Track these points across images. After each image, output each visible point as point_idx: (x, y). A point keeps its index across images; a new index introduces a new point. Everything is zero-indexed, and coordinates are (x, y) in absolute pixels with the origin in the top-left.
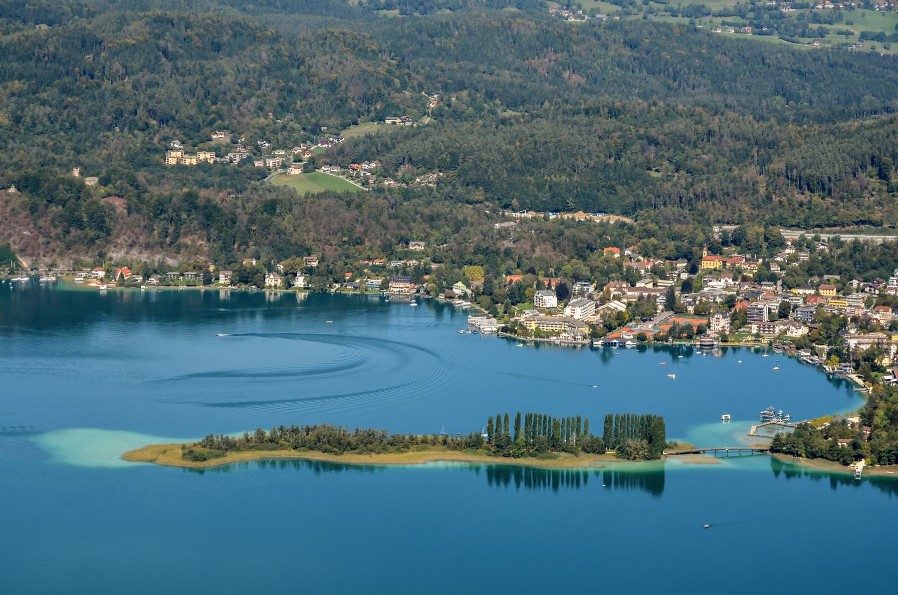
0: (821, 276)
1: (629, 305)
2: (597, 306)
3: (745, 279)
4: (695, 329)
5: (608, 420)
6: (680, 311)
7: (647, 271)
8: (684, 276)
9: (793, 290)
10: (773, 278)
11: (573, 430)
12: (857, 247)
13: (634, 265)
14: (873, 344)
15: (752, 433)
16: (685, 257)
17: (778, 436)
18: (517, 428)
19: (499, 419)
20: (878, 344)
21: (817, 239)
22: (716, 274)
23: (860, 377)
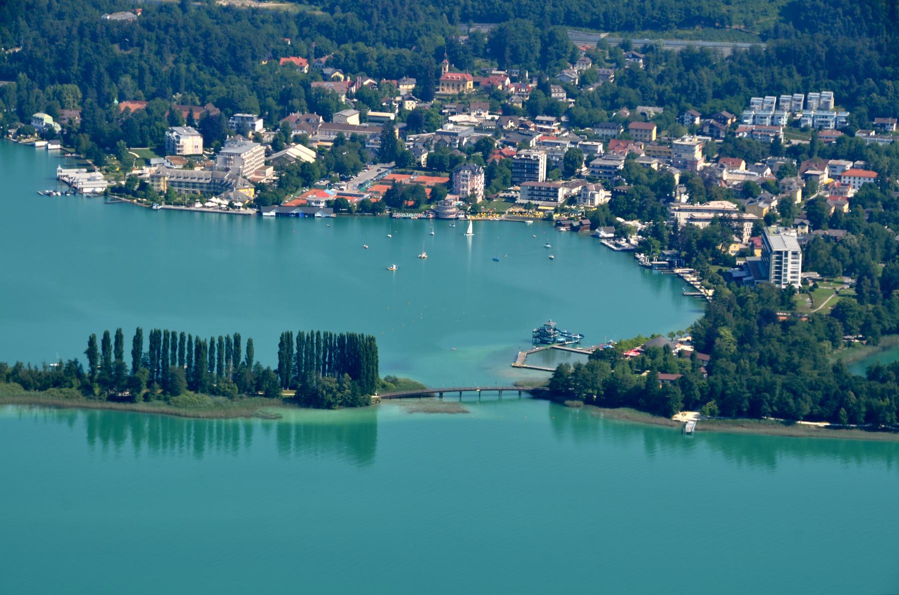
0: (631, 106)
1: (320, 152)
2: (268, 153)
3: (508, 111)
4: (428, 191)
5: (285, 341)
6: (404, 162)
7: (349, 96)
8: (410, 105)
10: (553, 110)
11: (228, 358)
12: (690, 60)
13: (327, 85)
14: (713, 221)
15: (518, 363)
18: (136, 353)
19: (106, 336)
20: (721, 219)
21: (626, 46)
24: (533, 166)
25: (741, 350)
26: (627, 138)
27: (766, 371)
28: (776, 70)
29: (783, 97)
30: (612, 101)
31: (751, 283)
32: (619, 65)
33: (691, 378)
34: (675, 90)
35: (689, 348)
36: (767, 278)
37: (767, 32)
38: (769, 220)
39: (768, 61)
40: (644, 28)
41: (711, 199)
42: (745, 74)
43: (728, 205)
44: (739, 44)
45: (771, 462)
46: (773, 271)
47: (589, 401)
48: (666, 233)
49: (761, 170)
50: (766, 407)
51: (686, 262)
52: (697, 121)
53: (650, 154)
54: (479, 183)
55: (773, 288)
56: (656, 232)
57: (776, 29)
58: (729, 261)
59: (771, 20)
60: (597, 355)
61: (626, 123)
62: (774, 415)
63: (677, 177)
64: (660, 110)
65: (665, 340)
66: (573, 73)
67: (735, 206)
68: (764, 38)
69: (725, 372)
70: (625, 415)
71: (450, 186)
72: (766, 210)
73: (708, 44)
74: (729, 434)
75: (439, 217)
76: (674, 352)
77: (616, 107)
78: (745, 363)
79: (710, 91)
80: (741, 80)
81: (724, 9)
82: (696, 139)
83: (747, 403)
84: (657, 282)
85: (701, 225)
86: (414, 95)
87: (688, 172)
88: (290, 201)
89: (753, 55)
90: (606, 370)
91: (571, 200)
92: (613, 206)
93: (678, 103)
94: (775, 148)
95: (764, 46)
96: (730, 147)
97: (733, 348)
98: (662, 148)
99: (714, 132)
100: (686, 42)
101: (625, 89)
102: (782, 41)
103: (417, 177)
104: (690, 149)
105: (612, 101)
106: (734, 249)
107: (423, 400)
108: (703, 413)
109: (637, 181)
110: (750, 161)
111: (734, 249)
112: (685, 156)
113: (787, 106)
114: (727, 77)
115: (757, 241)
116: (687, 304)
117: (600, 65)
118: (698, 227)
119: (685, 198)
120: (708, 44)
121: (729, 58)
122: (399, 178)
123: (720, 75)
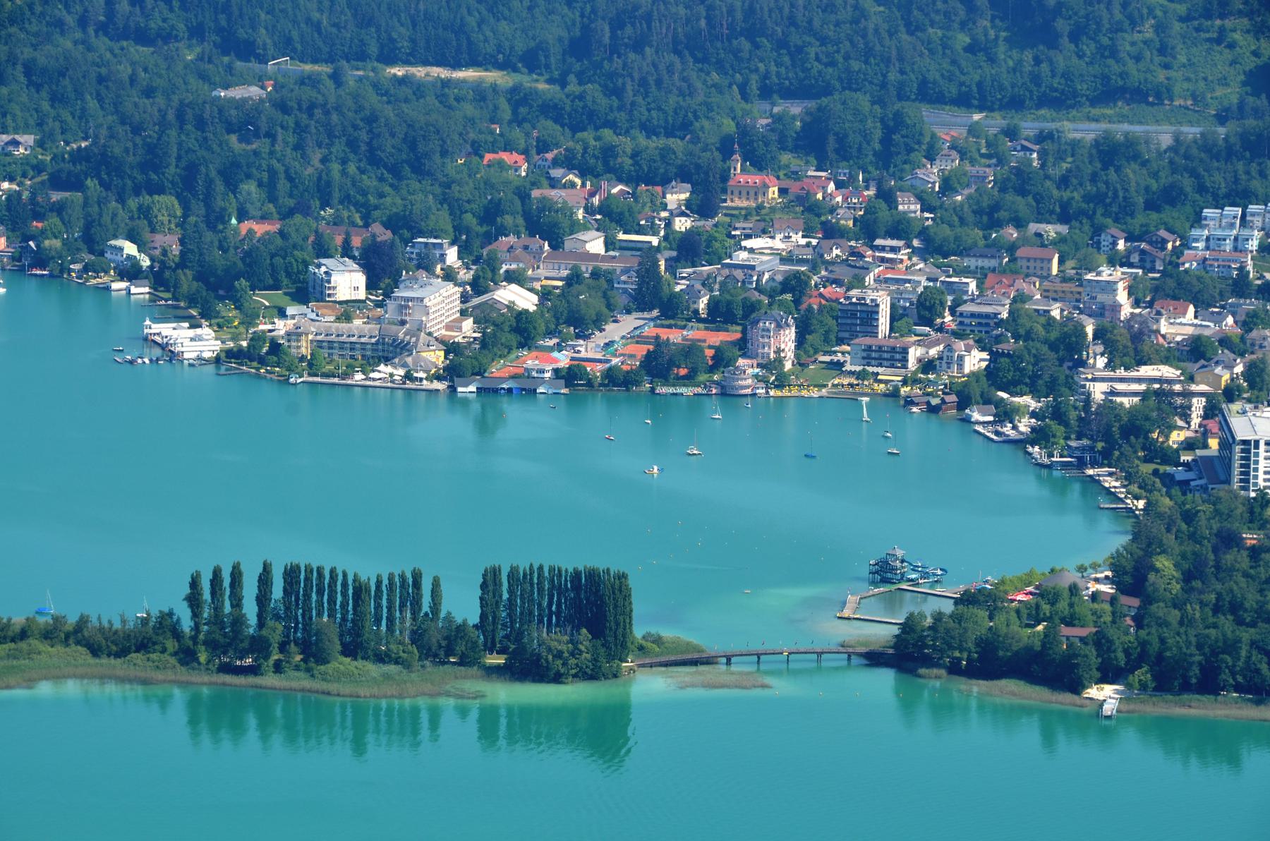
0: (1019, 224)
1: (545, 295)
2: (465, 298)
3: (832, 232)
4: (709, 353)
5: (490, 581)
7: (589, 210)
10: (899, 229)
11: (402, 606)
14: (1144, 395)
15: (846, 613)
16: (684, 175)
17: (910, 617)
18: (263, 599)
19: (217, 573)
20: (1157, 393)
24: (870, 314)
25: (1188, 590)
26: (1012, 271)
27: (1226, 622)
28: (1240, 166)
29: (1252, 208)
30: (990, 216)
31: (1204, 489)
32: (1001, 161)
33: (1112, 633)
34: (1087, 198)
35: (1106, 589)
36: (1228, 481)
37: (1227, 110)
38: (1230, 394)
39: (1228, 153)
40: (1039, 106)
41: (1141, 362)
42: (1194, 174)
43: (1167, 371)
44: (1185, 129)
45: (1234, 761)
46: (1236, 470)
47: (955, 669)
48: (1073, 415)
49: (1217, 320)
50: (1225, 676)
51: (1104, 458)
52: (1121, 245)
53: (1048, 296)
54: (787, 340)
55: (1236, 497)
56: (1057, 414)
57: (1241, 106)
58: (1169, 457)
59: (1231, 94)
60: (967, 599)
61: (1012, 248)
62: (1238, 688)
63: (1090, 330)
64: (1064, 229)
65: (1073, 577)
66: (931, 175)
67: (1178, 372)
68: (1222, 119)
69: (1163, 623)
70: (1011, 690)
71: (743, 346)
72: (1226, 377)
73: (1137, 129)
74: (1169, 719)
75: (727, 393)
76: (1086, 595)
77: (997, 224)
78: (1194, 610)
79: (1140, 200)
80: (1187, 183)
81: (1161, 76)
82: (1119, 272)
83: (1196, 670)
84: (1060, 488)
85: (1126, 402)
86: (691, 208)
87: (1106, 321)
88: (498, 369)
89: (1206, 145)
90: (981, 621)
91: (927, 366)
92: (991, 374)
93: (1091, 218)
94: (1240, 286)
95: (1222, 131)
96: (1171, 283)
97: (1176, 588)
98: (1067, 287)
99: (1146, 262)
100: (1104, 126)
101: (1010, 197)
102: (1251, 123)
103: (693, 333)
104: (1110, 287)
105: (990, 216)
106: (1176, 437)
107: (702, 668)
108: (1129, 686)
109: (1028, 336)
110: (1202, 304)
111: (1176, 437)
112: (1101, 298)
113: (1258, 221)
114: (1165, 178)
115: (1213, 425)
116: (1105, 522)
117: (973, 162)
118: (1121, 404)
119: (1101, 362)
120: (1137, 129)
121: (1169, 149)
122: (664, 334)
123: (1155, 175)
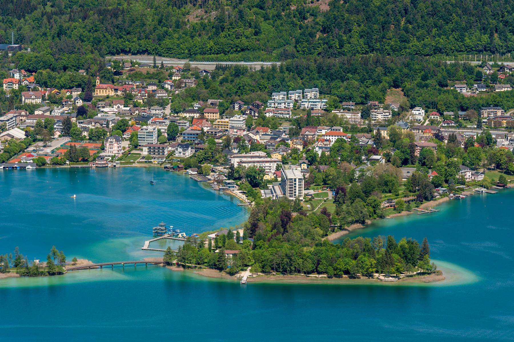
9: (180, 114)
15: (145, 247)
16: (79, 86)
22: (109, 101)
23: (244, 193)
67: (265, 154)
118: (245, 167)
121: (259, 71)
